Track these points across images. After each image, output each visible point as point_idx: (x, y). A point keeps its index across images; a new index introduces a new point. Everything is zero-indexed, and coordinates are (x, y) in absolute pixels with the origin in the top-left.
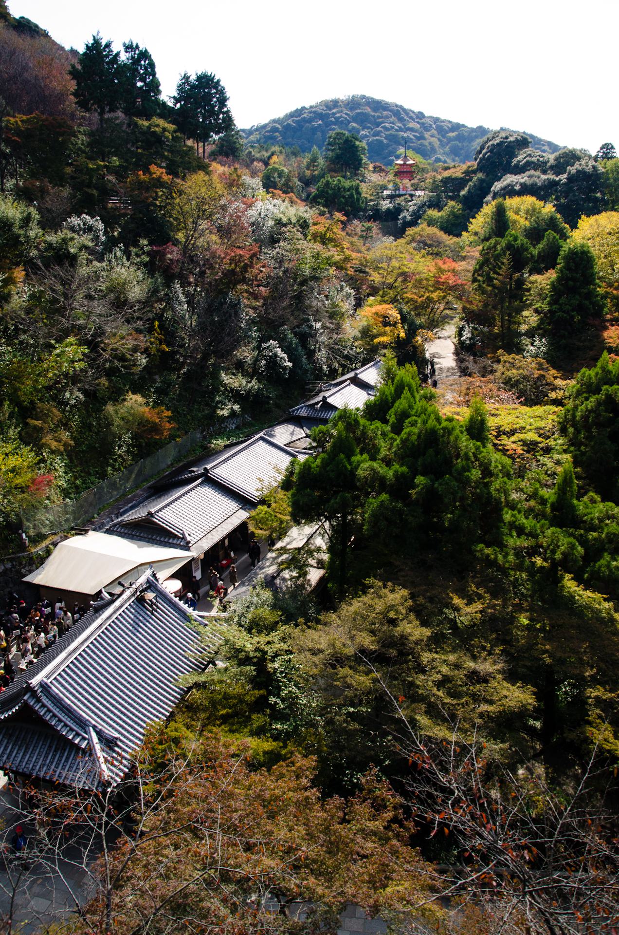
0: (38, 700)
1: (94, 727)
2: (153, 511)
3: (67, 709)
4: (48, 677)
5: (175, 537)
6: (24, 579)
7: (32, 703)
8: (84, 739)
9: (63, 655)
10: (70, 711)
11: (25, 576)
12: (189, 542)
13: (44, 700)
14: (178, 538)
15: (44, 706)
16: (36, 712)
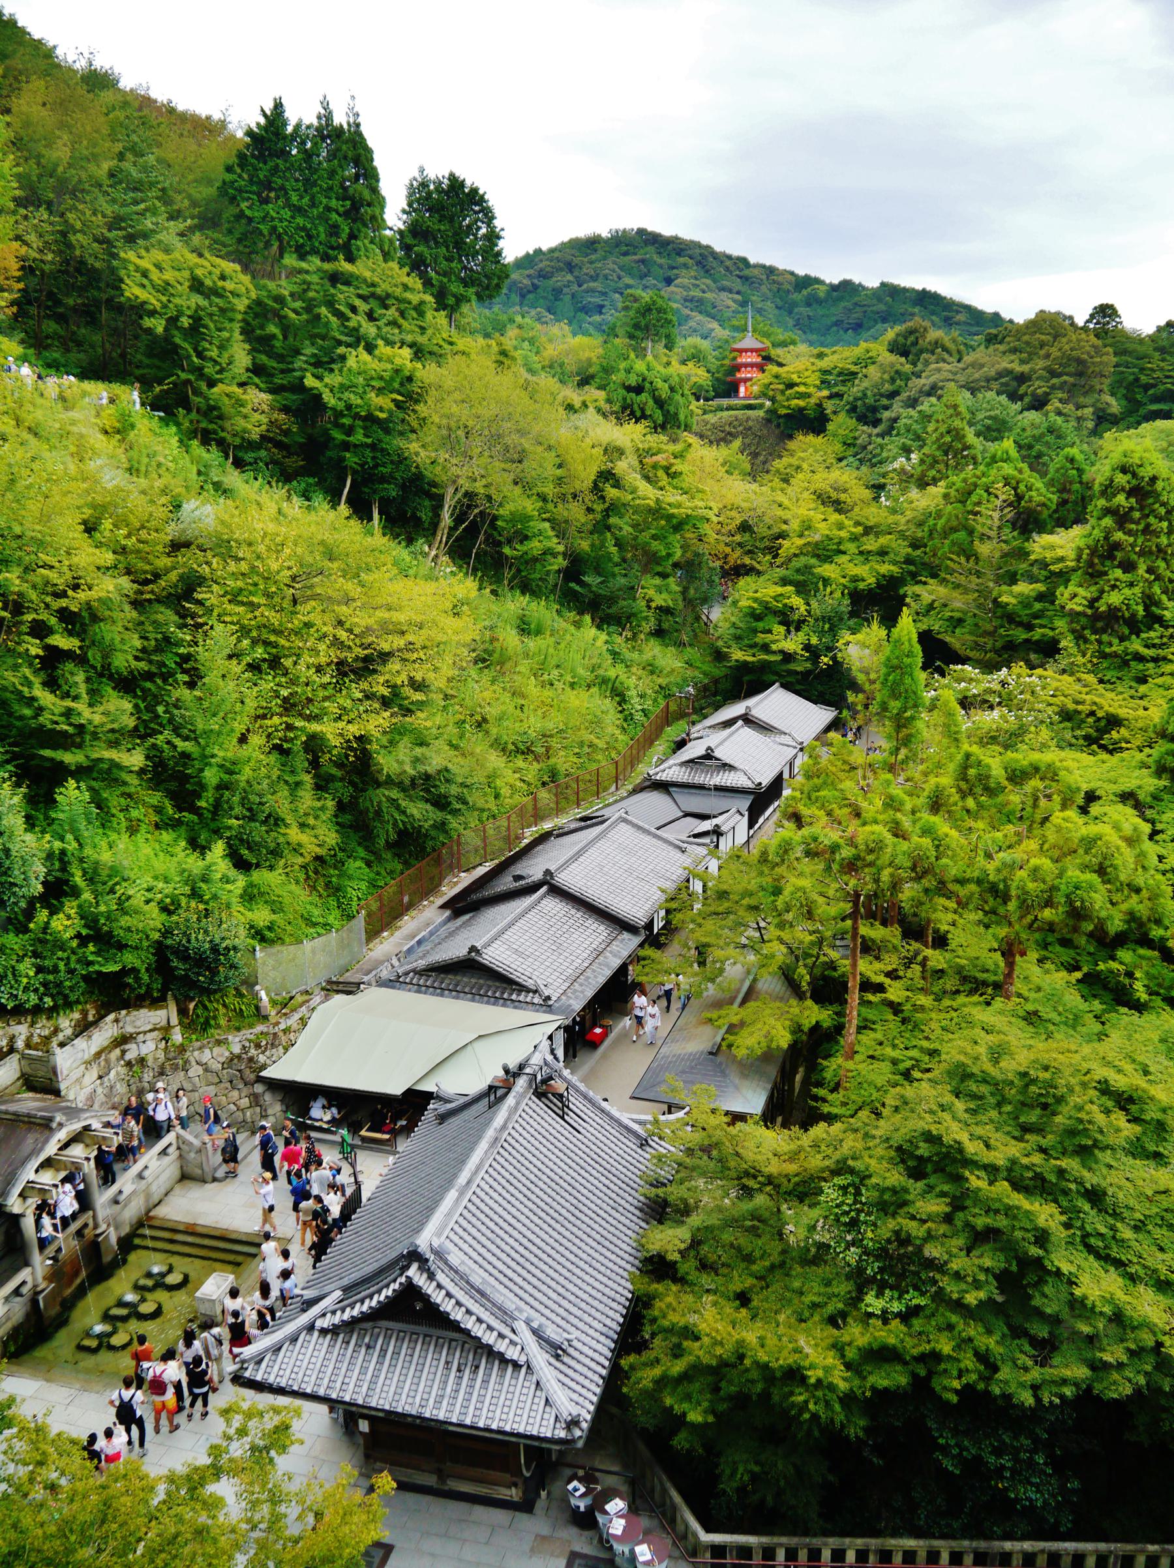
0: (431, 1277)
1: (527, 1323)
2: (478, 945)
3: (478, 1291)
4: (438, 1234)
5: (522, 988)
6: (264, 1074)
7: (420, 1280)
8: (512, 1342)
9: (452, 1194)
10: (482, 1294)
11: (264, 1067)
12: (549, 998)
13: (440, 1277)
14: (528, 991)
15: (439, 1286)
16: (425, 1298)
